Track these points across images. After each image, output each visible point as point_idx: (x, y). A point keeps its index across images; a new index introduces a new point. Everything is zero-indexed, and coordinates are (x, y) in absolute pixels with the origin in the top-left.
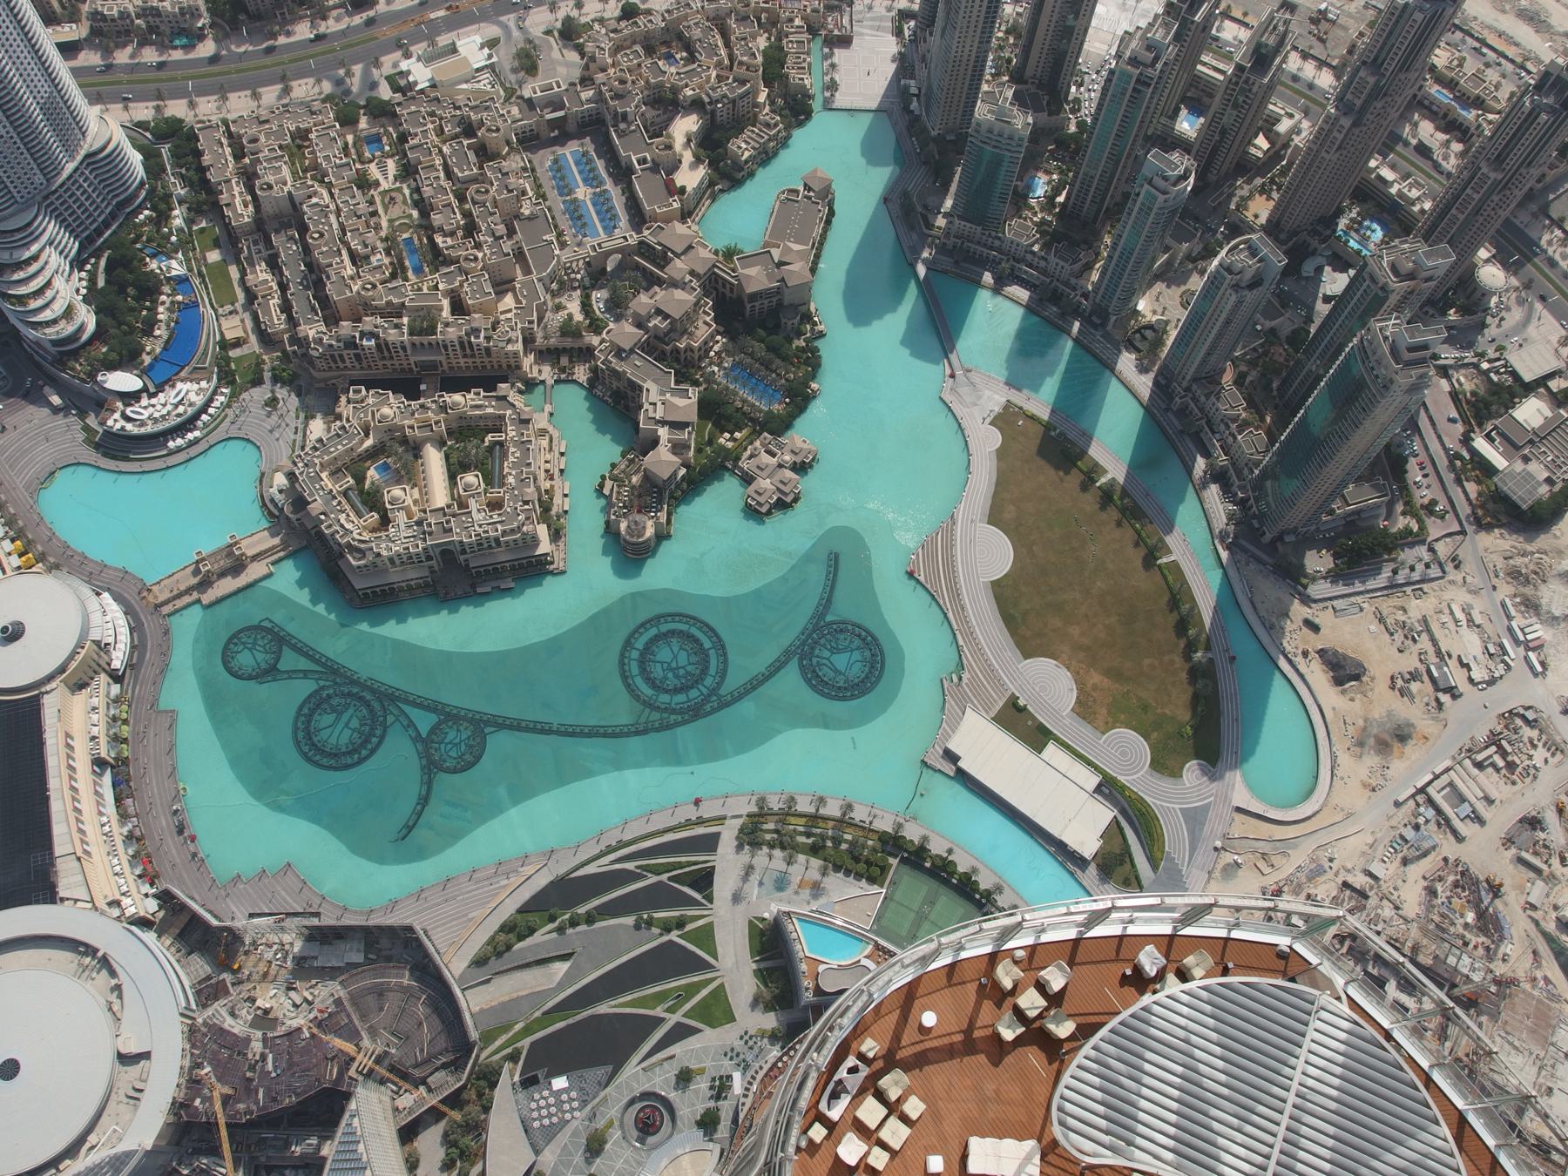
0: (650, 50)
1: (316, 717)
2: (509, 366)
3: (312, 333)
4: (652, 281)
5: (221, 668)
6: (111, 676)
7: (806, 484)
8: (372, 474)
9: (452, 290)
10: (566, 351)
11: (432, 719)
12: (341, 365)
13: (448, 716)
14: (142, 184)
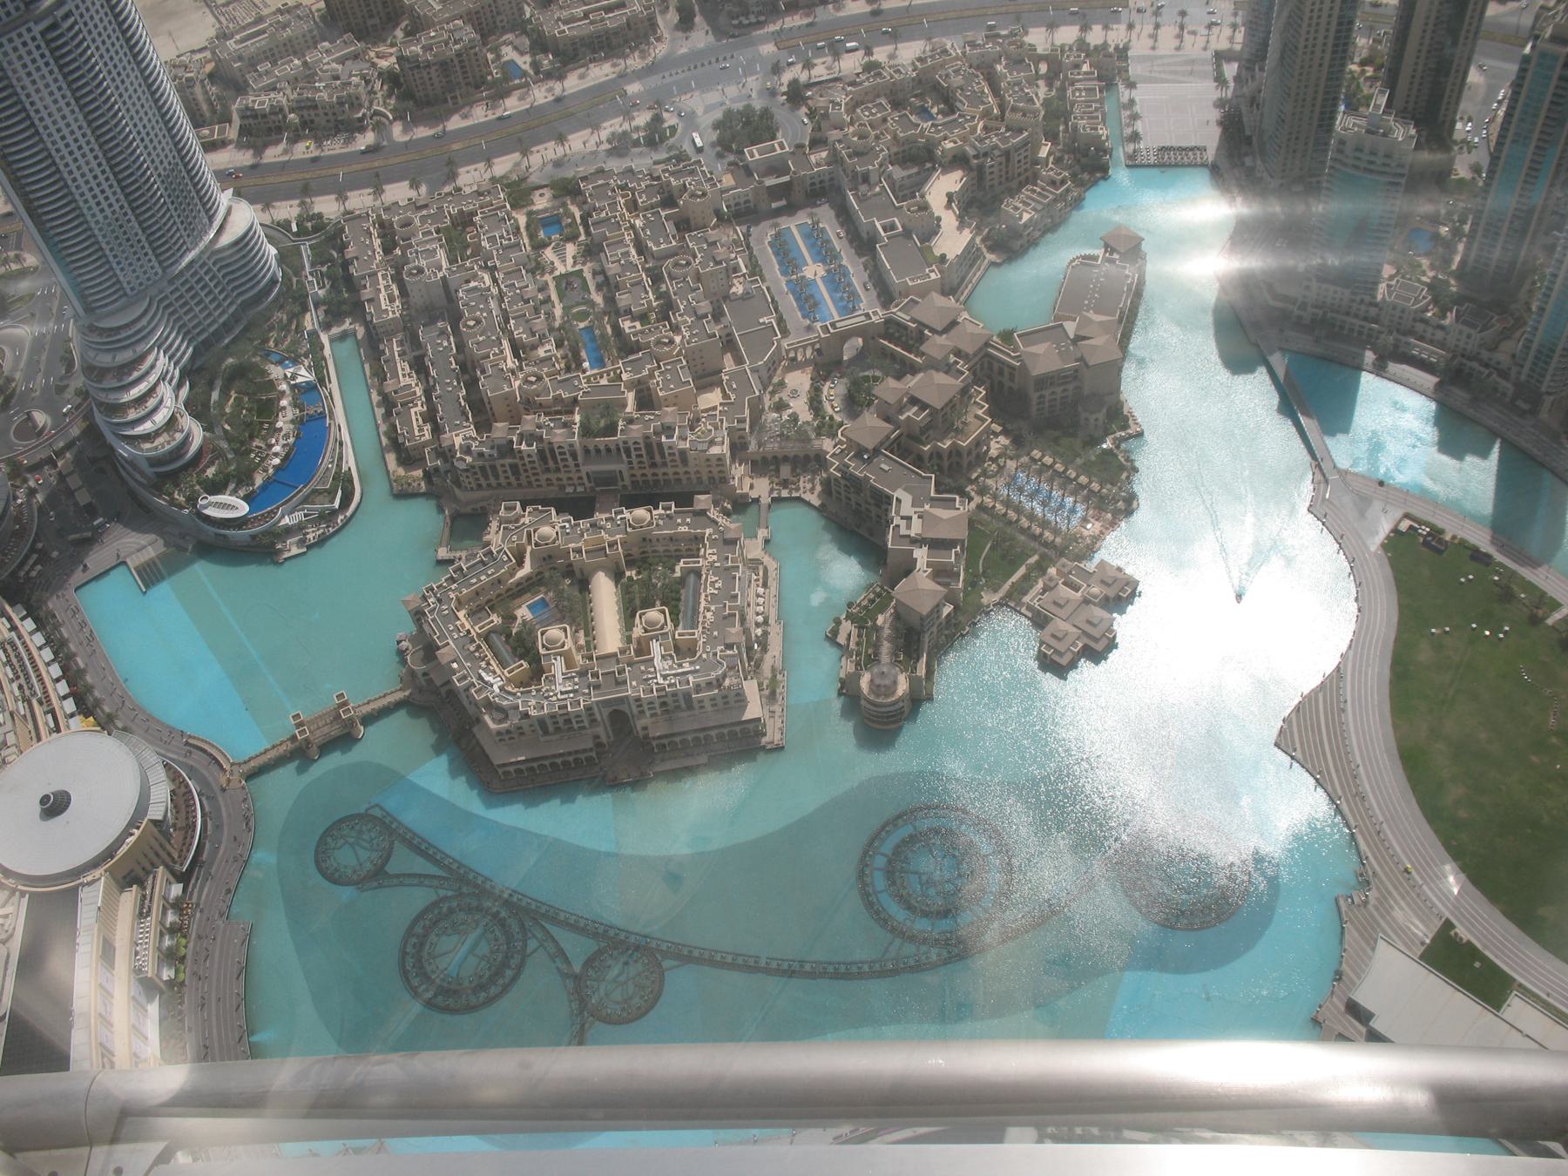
0: (896, 105)
1: (433, 938)
2: (712, 479)
3: (458, 441)
4: (904, 369)
5: (312, 866)
6: (173, 872)
7: (1125, 625)
8: (523, 613)
9: (639, 381)
10: (789, 462)
11: (590, 946)
12: (493, 481)
13: (614, 943)
14: (273, 281)
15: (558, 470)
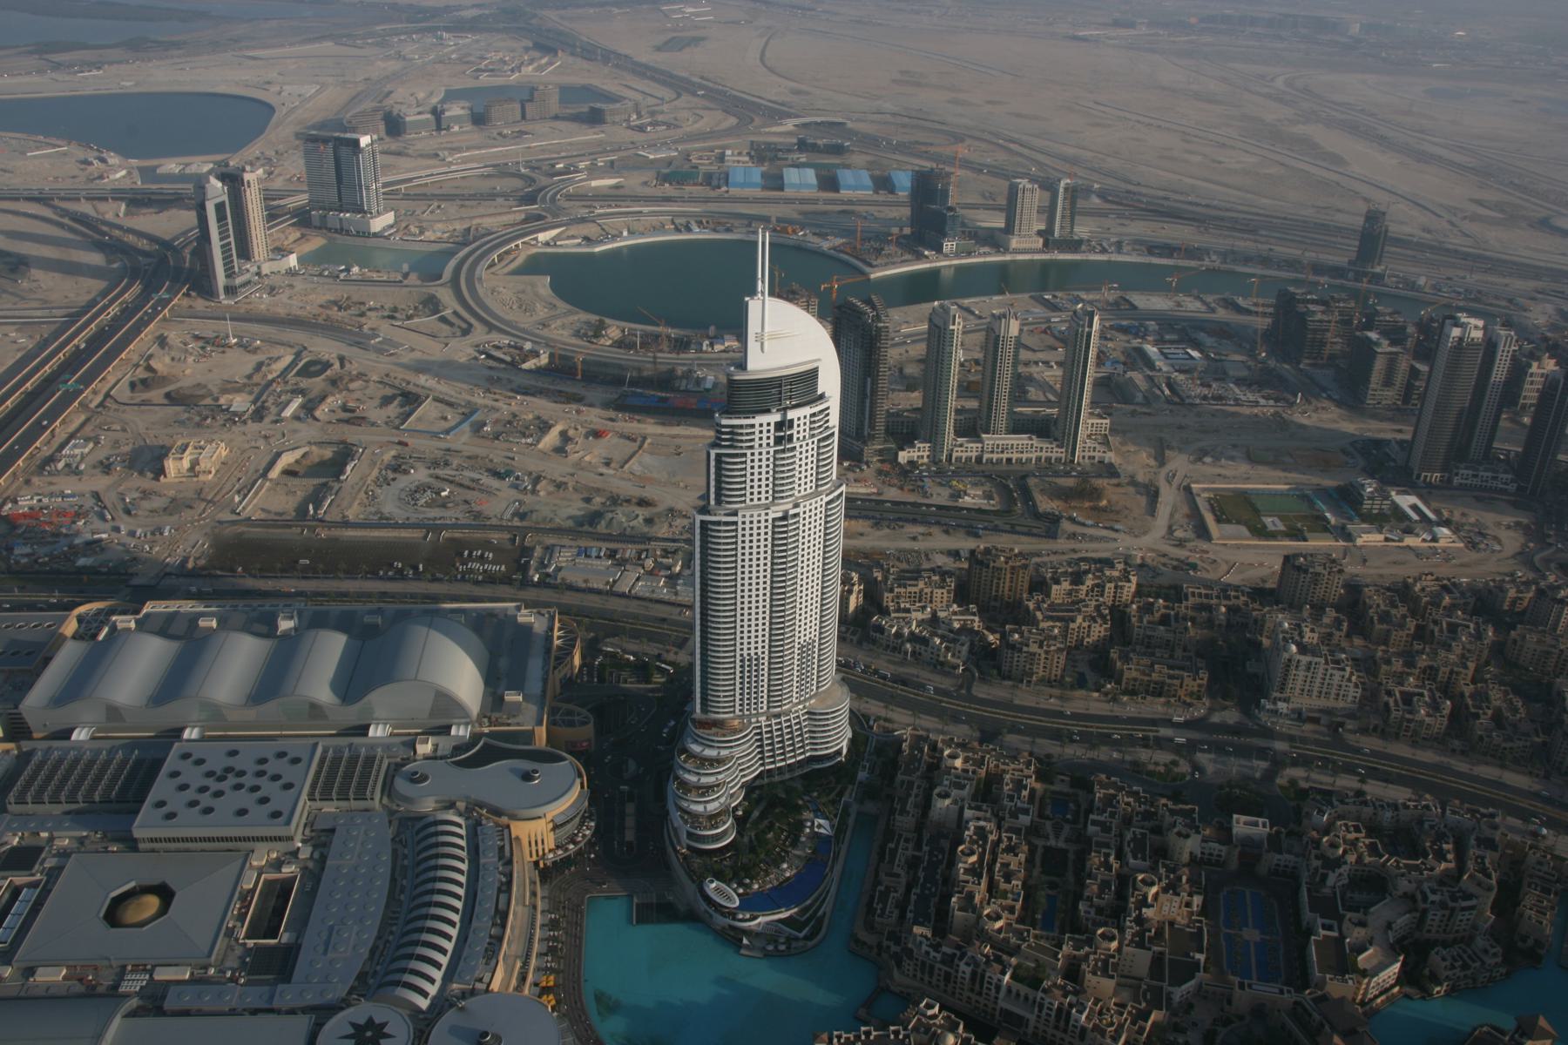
12: (926, 978)
14: (839, 753)
15: (980, 994)
